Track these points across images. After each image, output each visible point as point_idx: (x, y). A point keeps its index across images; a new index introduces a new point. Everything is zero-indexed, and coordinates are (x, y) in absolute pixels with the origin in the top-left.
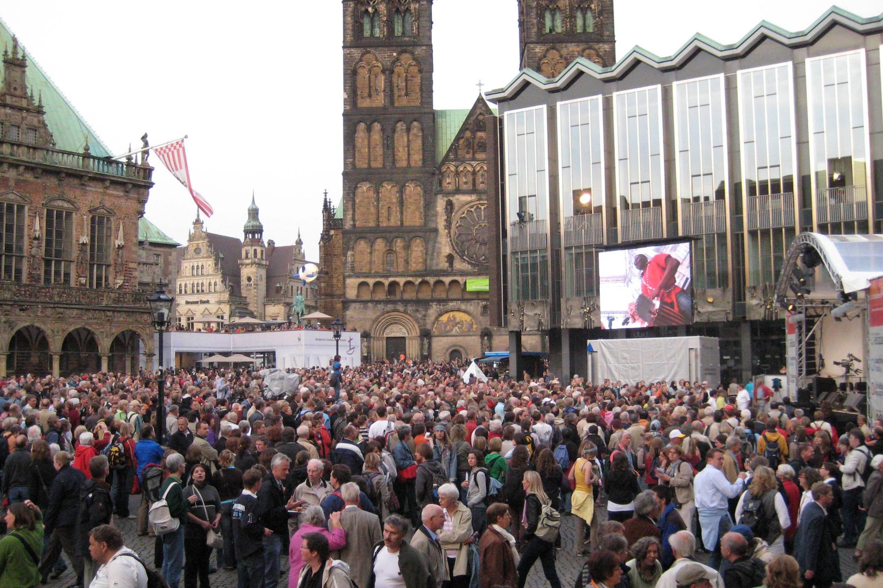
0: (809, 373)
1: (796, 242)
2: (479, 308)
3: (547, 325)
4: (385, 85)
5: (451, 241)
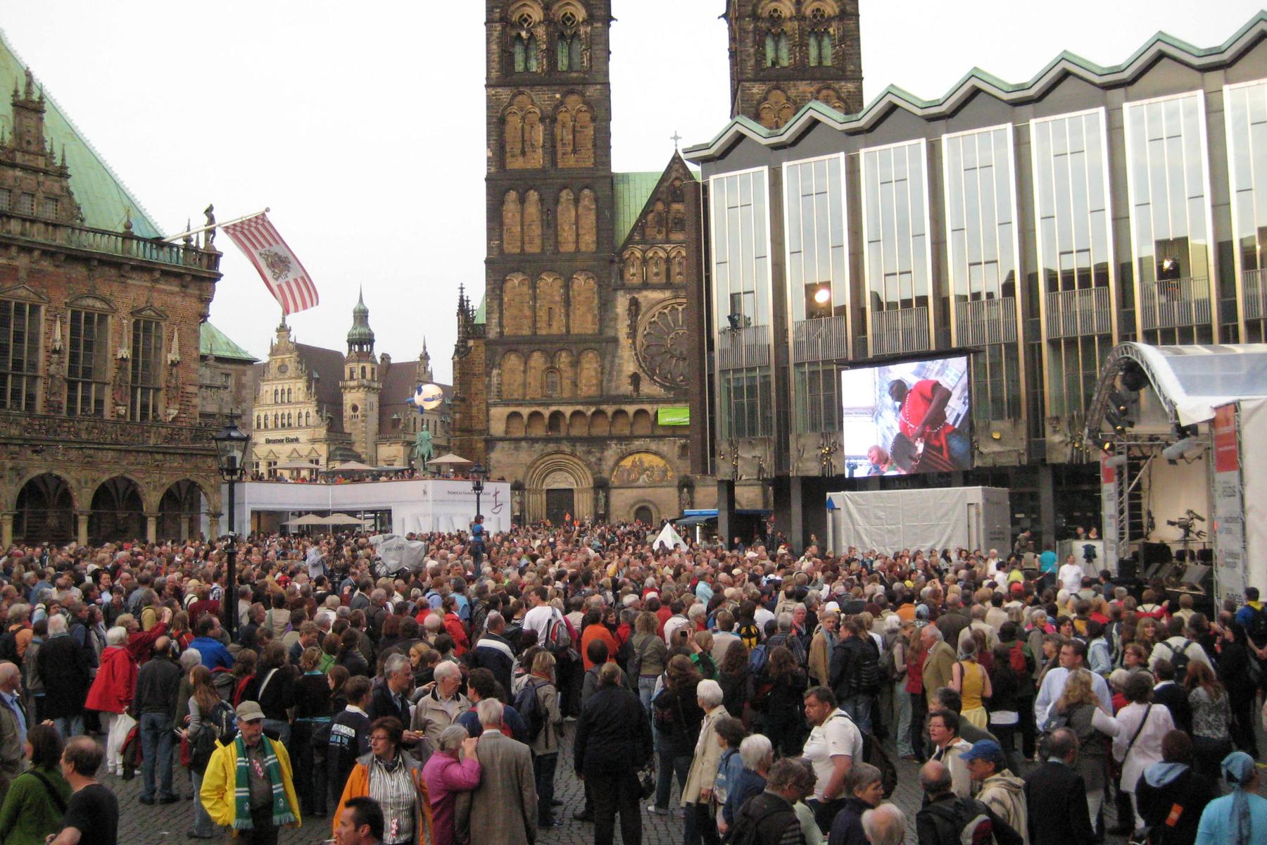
0: (1133, 537)
1: (1113, 355)
2: (676, 449)
3: (770, 472)
4: (544, 138)
5: (636, 354)
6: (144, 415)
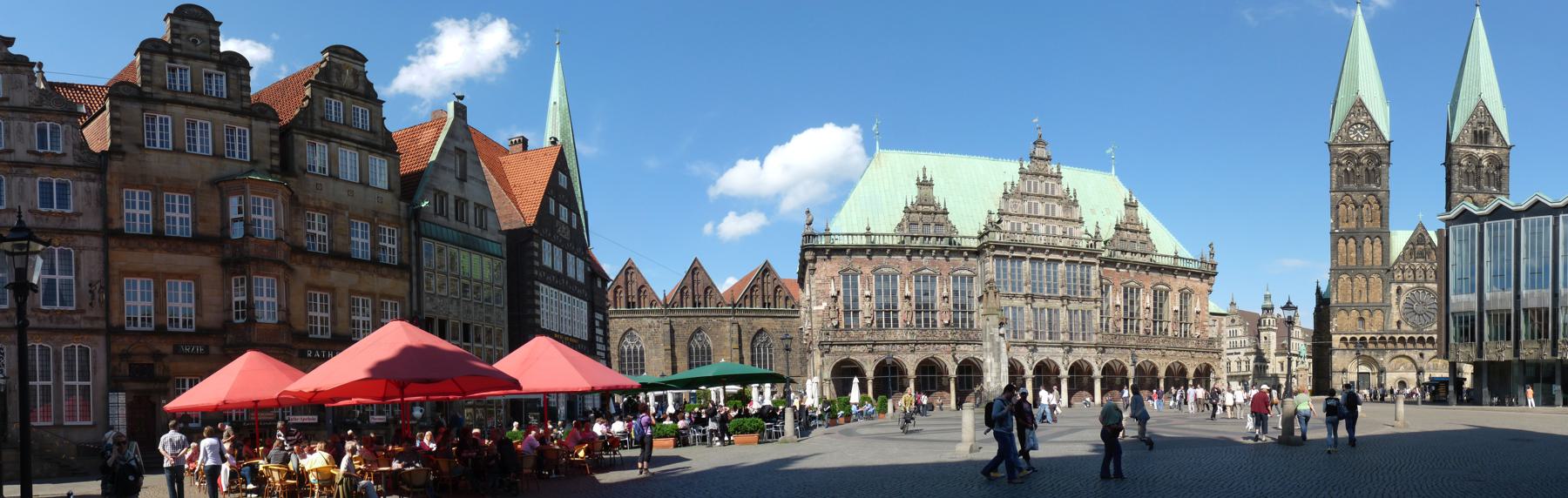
6: (1185, 336)
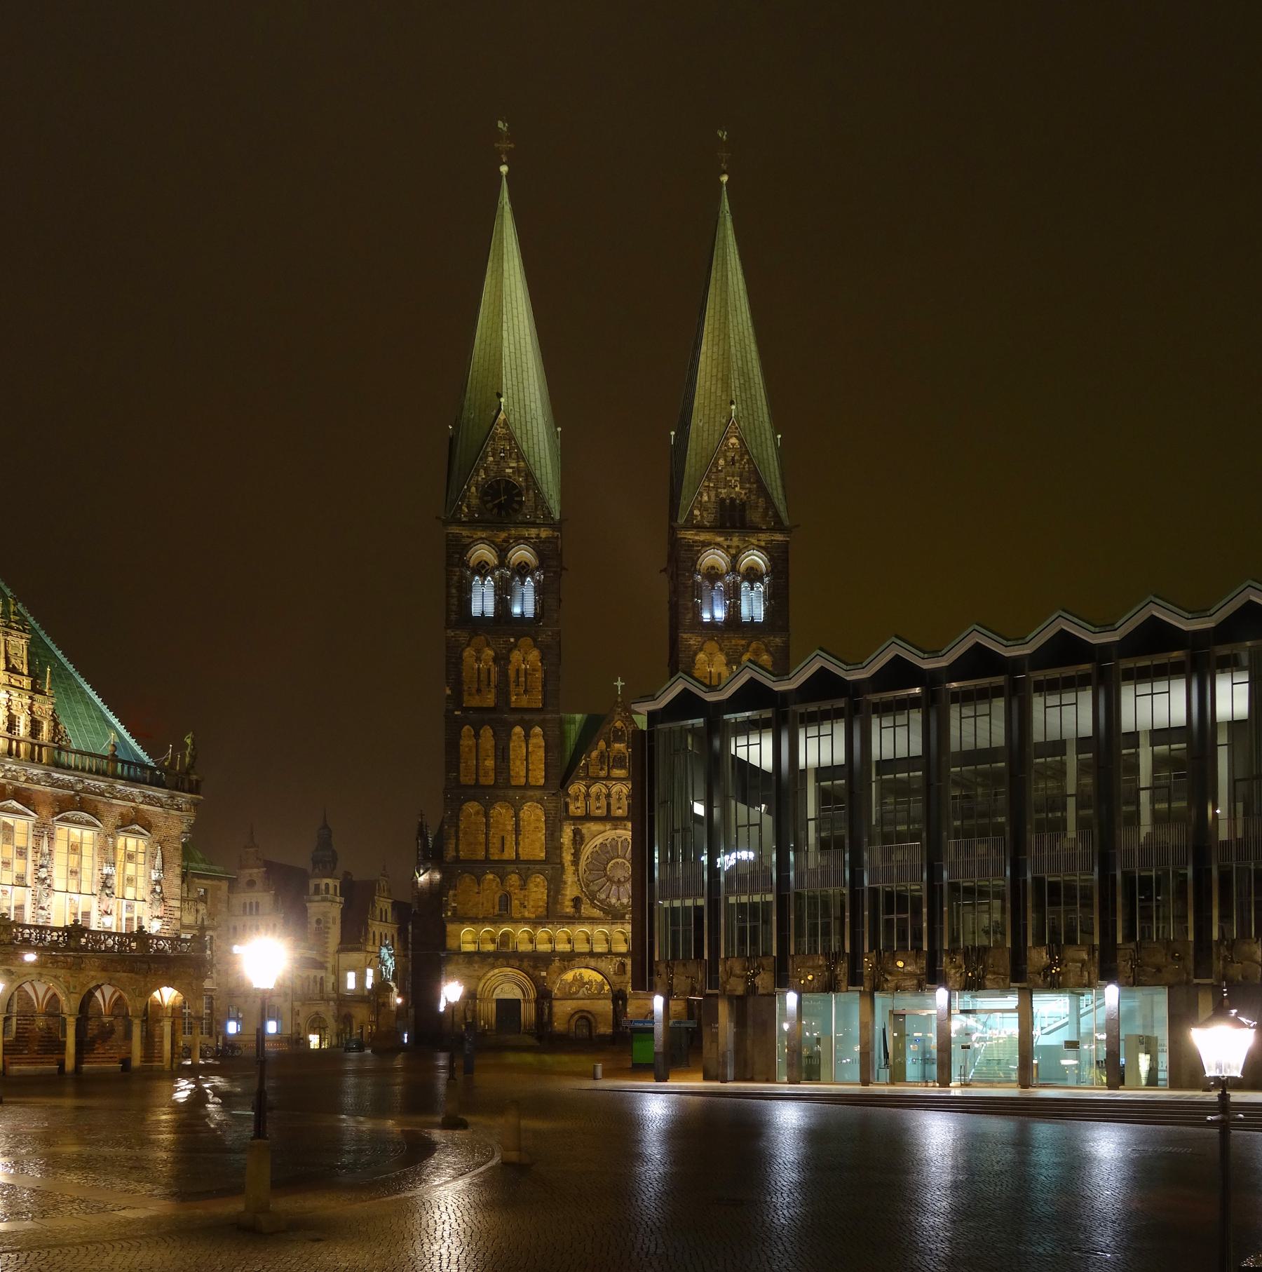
5: (579, 880)
